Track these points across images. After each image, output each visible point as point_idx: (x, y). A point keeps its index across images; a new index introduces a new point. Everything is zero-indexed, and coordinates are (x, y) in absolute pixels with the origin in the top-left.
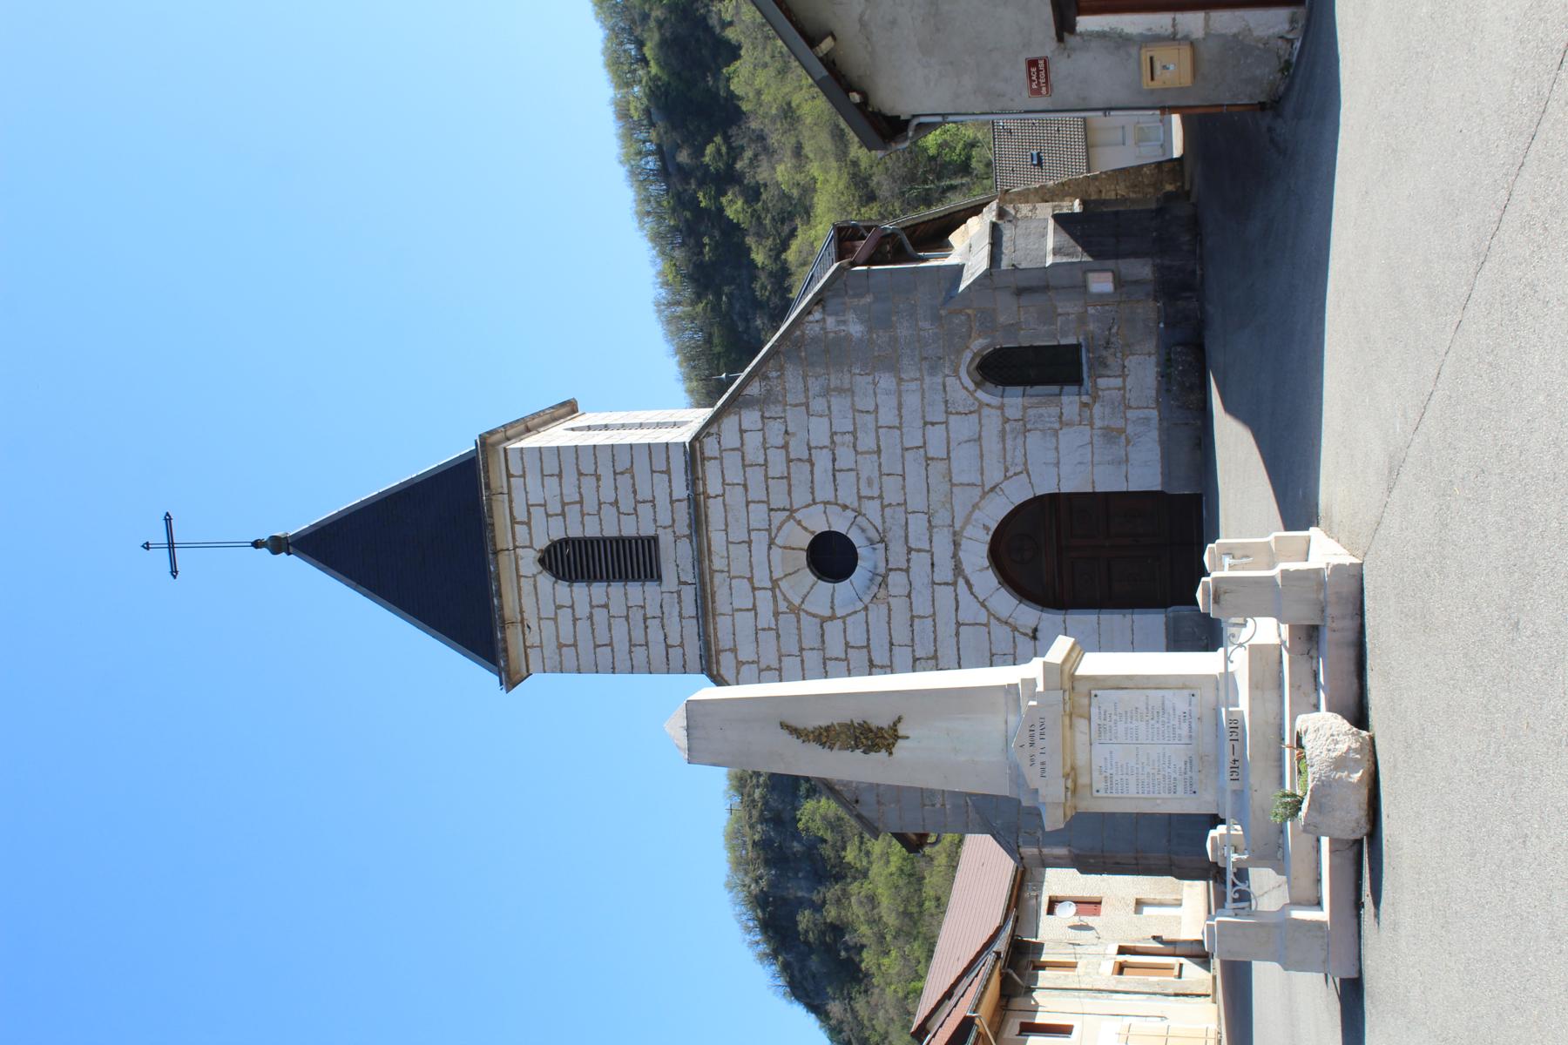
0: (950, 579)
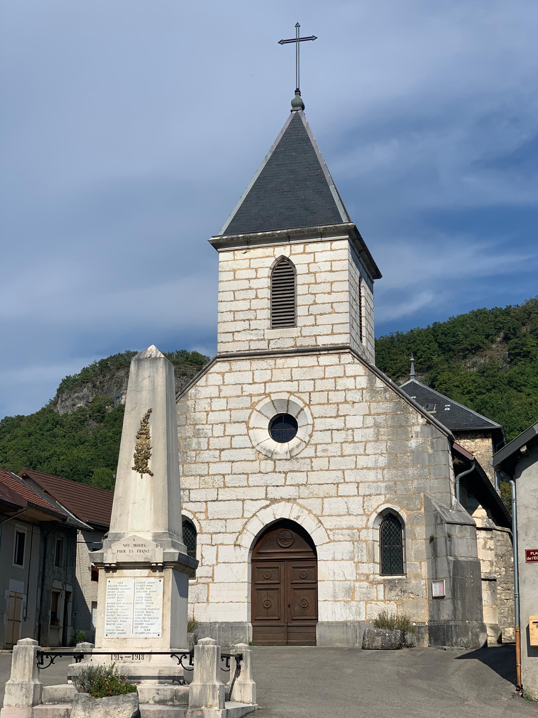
0: (270, 496)
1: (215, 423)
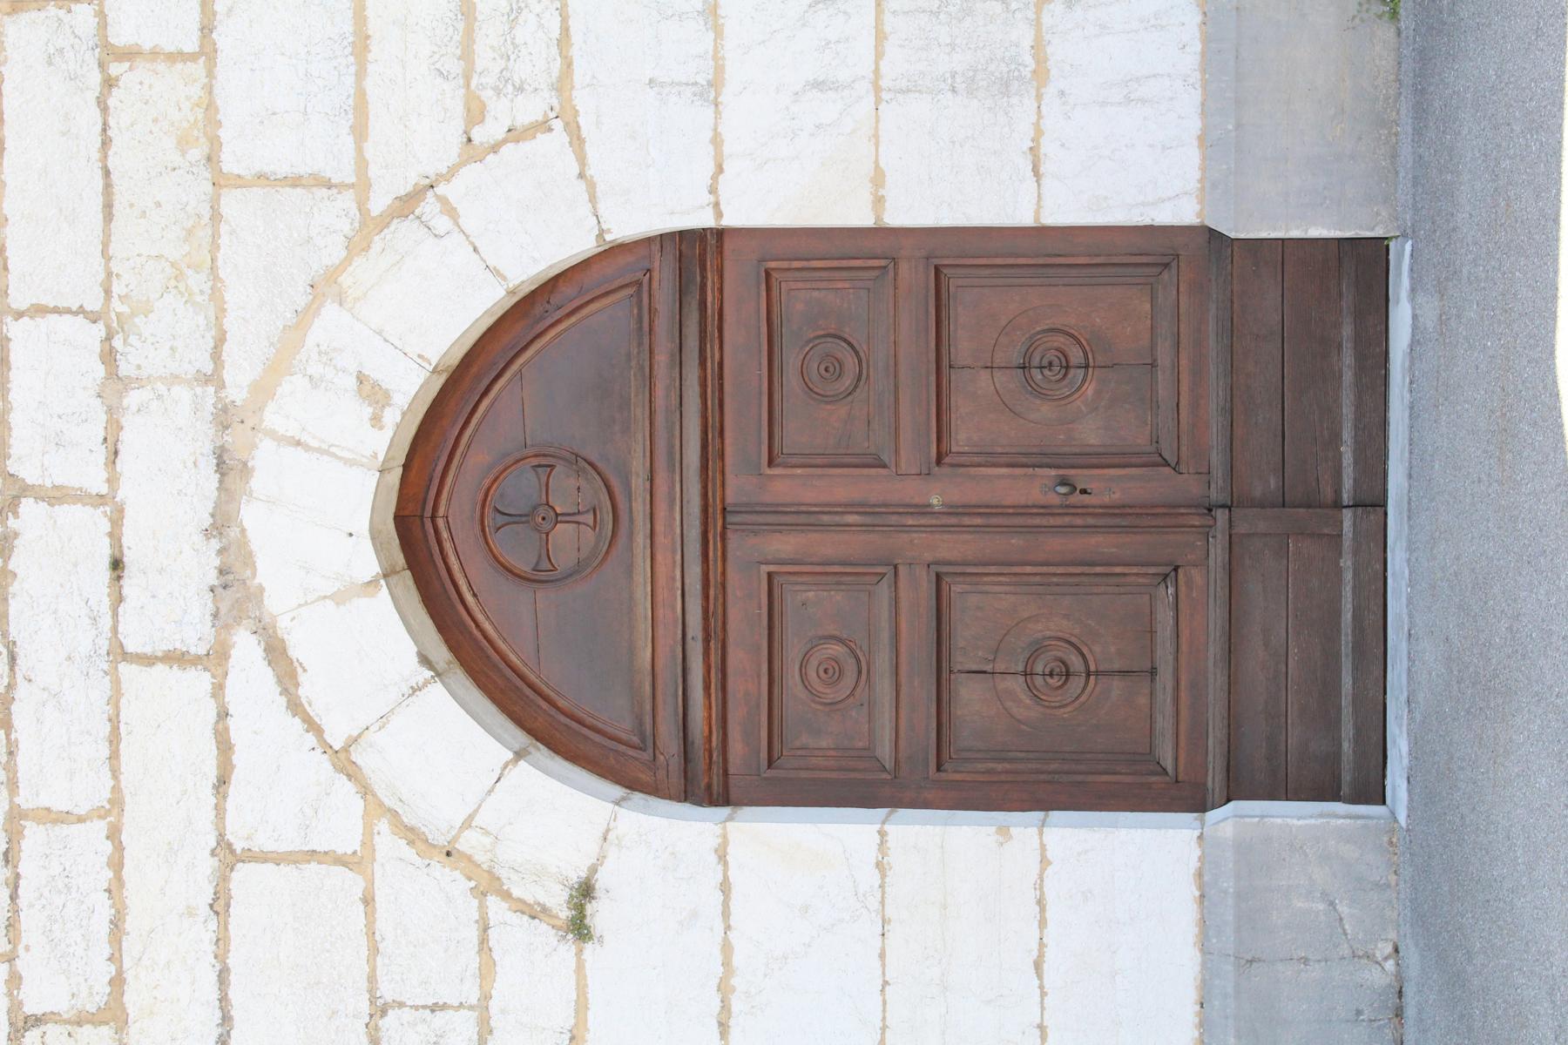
0: (195, 634)
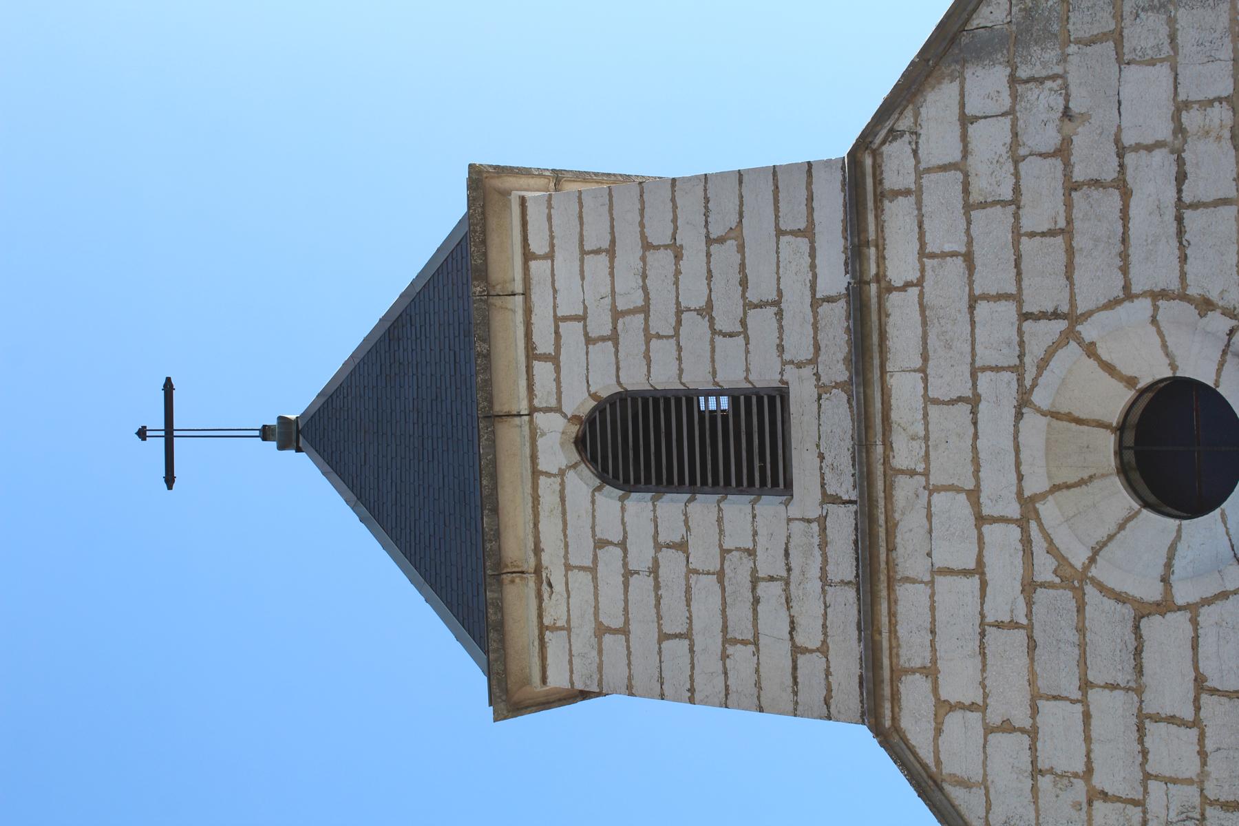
1: (1142, 765)
